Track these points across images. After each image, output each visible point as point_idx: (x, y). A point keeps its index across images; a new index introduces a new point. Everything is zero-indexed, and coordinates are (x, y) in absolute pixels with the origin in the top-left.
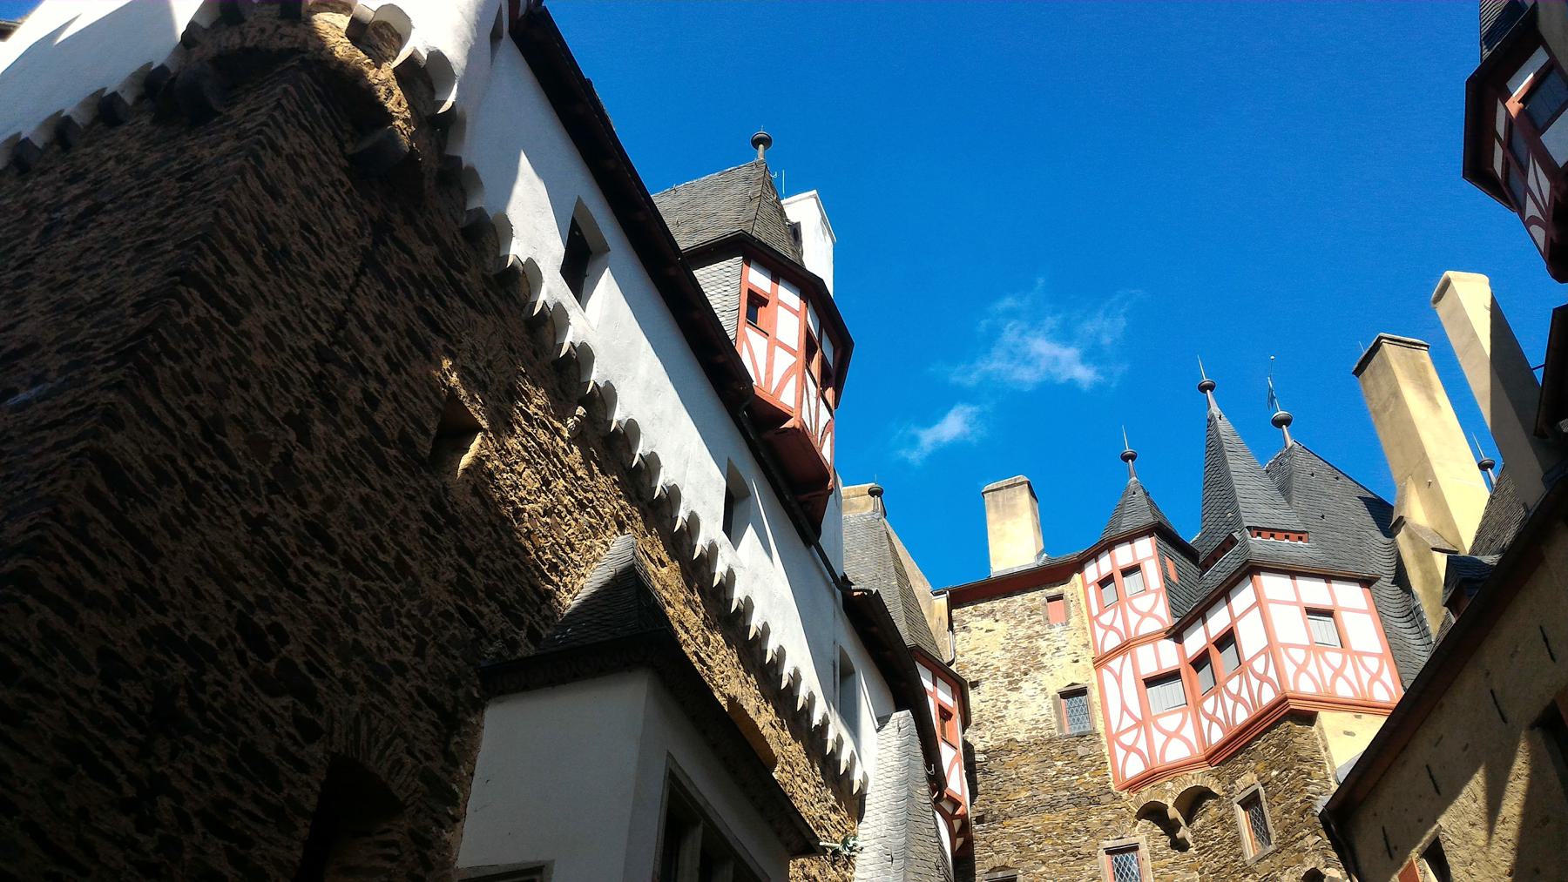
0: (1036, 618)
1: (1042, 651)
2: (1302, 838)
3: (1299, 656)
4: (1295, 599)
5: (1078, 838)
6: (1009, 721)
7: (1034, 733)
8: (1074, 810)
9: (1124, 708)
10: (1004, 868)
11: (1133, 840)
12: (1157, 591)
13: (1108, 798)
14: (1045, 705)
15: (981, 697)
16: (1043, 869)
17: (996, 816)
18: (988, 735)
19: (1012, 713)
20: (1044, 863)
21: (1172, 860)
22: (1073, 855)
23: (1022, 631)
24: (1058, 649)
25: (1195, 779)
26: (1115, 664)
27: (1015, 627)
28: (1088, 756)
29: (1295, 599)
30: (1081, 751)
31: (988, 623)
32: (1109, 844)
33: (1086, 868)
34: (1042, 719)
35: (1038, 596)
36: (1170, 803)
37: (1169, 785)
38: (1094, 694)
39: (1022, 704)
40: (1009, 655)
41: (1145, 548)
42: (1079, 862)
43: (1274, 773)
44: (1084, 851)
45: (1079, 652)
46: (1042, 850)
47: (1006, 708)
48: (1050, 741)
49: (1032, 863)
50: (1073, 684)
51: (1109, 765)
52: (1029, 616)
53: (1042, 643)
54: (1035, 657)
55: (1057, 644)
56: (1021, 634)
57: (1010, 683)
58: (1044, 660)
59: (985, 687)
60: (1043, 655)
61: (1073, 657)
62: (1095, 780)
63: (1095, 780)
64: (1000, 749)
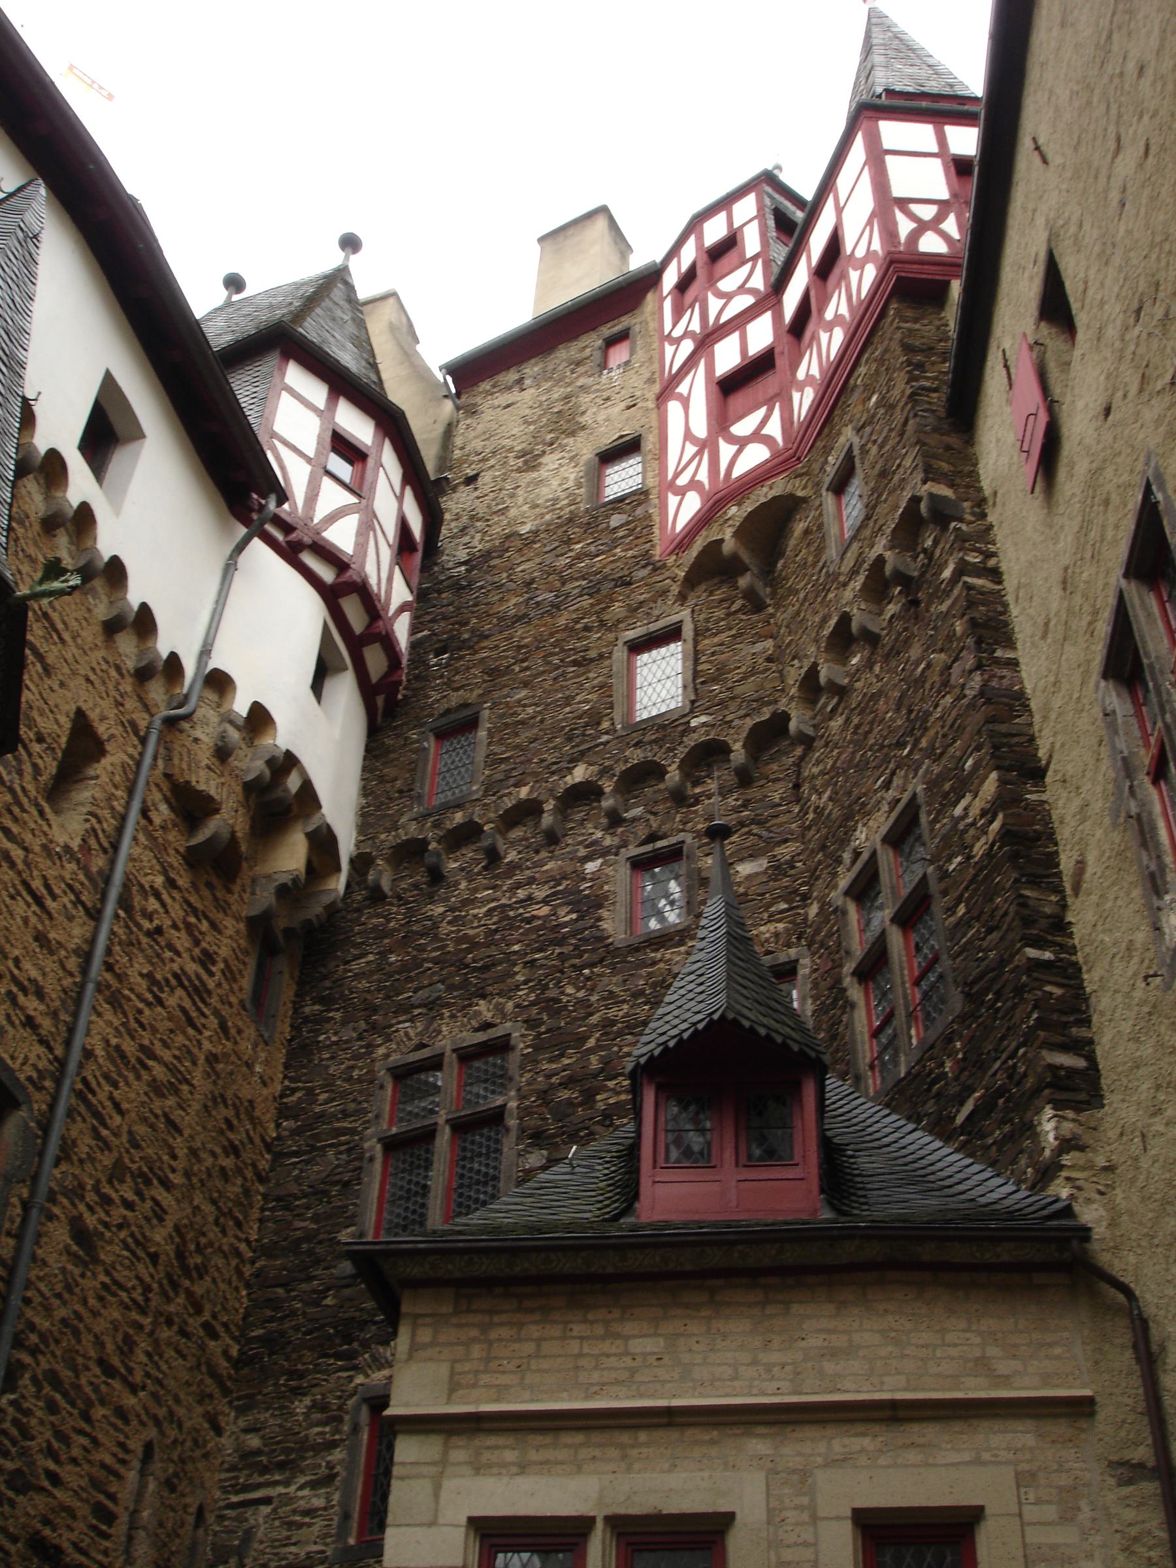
0: (581, 369)
1: (583, 409)
2: (899, 466)
3: (927, 212)
4: (935, 149)
5: (587, 638)
6: (513, 512)
7: (548, 517)
8: (586, 602)
9: (688, 436)
10: (465, 705)
11: (675, 618)
12: (754, 258)
13: (644, 572)
14: (572, 477)
15: (477, 493)
16: (523, 693)
17: (465, 641)
18: (478, 536)
19: (520, 500)
20: (526, 684)
21: (733, 632)
22: (575, 663)
23: (558, 392)
24: (608, 399)
25: (778, 487)
26: (683, 389)
27: (549, 390)
28: (628, 523)
29: (935, 149)
30: (616, 520)
31: (513, 396)
32: (631, 634)
33: (591, 675)
34: (563, 495)
35: (592, 341)
36: (728, 534)
37: (734, 509)
38: (649, 443)
39: (540, 482)
40: (532, 427)
41: (746, 208)
42: (582, 670)
43: (874, 399)
44: (593, 654)
45: (638, 394)
46: (527, 668)
47: (512, 496)
48: (570, 520)
49: (505, 691)
50: (621, 437)
51: (656, 530)
52: (573, 372)
53: (585, 399)
54: (573, 416)
55: (605, 395)
56: (556, 396)
57: (526, 462)
58: (585, 419)
59: (486, 479)
60: (583, 413)
61: (629, 402)
62: (630, 553)
63: (630, 553)
64: (489, 552)
